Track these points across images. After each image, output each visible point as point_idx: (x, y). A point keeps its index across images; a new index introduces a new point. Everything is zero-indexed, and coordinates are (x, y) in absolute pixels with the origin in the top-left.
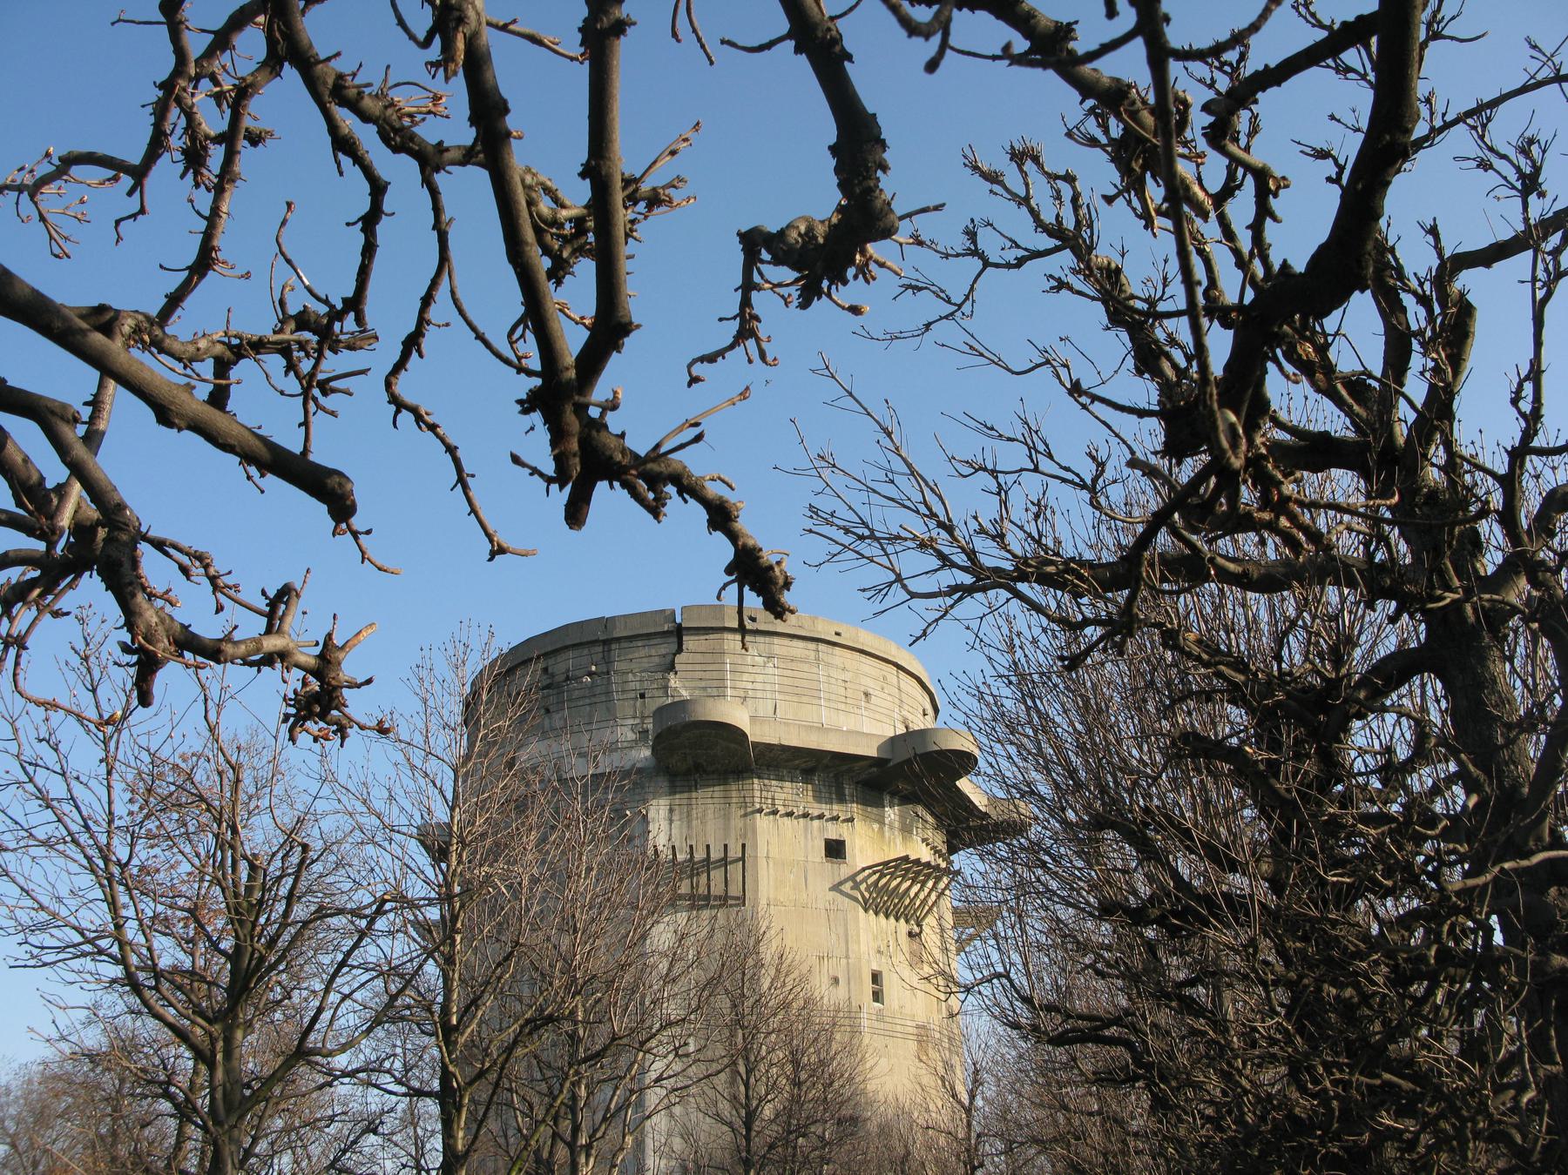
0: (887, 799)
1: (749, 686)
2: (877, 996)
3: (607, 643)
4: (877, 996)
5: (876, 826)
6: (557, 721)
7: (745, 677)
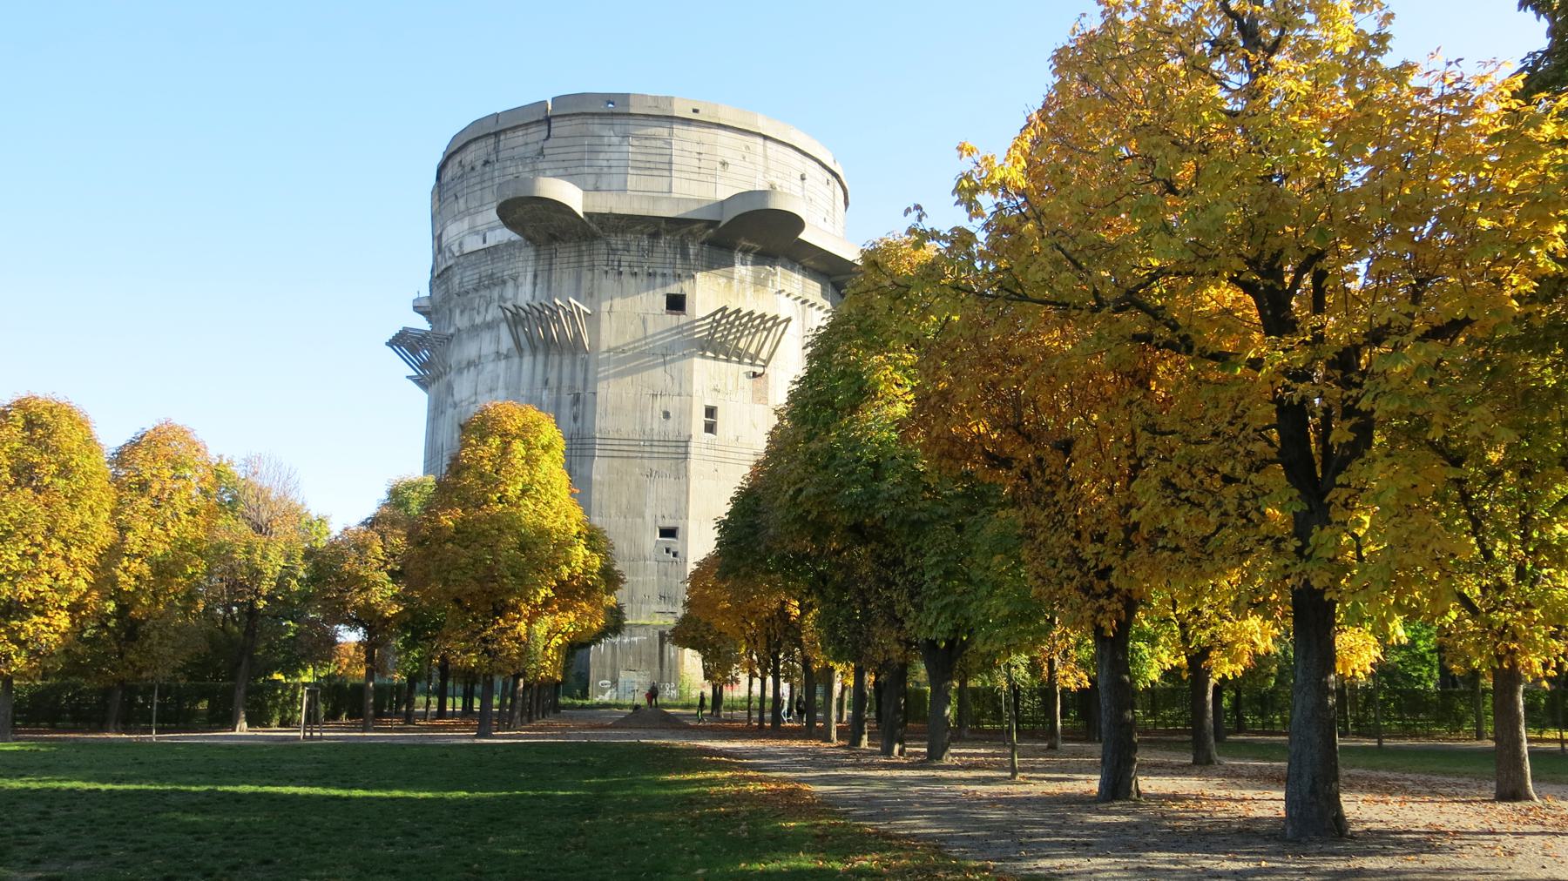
0: (738, 256)
1: (605, 163)
2: (710, 428)
3: (497, 134)
4: (710, 428)
5: (723, 281)
7: (602, 156)
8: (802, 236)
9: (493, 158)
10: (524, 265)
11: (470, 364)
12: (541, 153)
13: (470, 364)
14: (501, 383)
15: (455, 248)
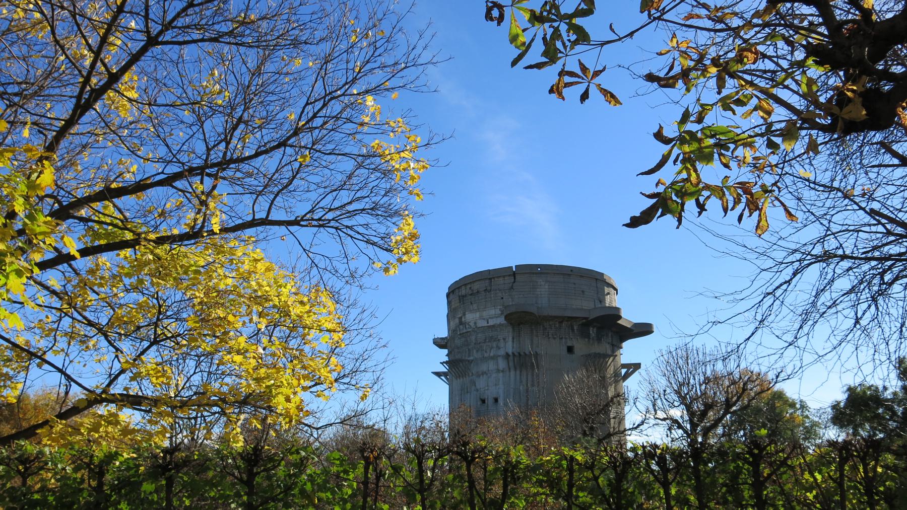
3: (490, 279)
6: (475, 306)
8: (619, 322)
9: (489, 288)
10: (508, 333)
11: (483, 373)
12: (512, 288)
13: (483, 373)
14: (501, 382)
15: (472, 324)
